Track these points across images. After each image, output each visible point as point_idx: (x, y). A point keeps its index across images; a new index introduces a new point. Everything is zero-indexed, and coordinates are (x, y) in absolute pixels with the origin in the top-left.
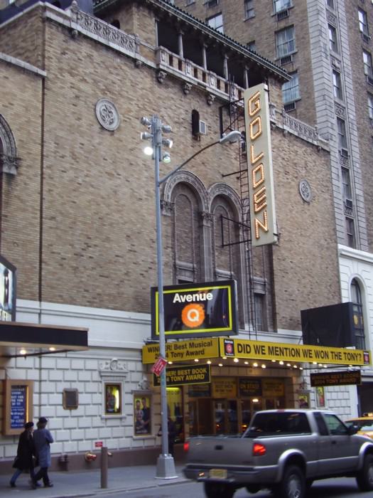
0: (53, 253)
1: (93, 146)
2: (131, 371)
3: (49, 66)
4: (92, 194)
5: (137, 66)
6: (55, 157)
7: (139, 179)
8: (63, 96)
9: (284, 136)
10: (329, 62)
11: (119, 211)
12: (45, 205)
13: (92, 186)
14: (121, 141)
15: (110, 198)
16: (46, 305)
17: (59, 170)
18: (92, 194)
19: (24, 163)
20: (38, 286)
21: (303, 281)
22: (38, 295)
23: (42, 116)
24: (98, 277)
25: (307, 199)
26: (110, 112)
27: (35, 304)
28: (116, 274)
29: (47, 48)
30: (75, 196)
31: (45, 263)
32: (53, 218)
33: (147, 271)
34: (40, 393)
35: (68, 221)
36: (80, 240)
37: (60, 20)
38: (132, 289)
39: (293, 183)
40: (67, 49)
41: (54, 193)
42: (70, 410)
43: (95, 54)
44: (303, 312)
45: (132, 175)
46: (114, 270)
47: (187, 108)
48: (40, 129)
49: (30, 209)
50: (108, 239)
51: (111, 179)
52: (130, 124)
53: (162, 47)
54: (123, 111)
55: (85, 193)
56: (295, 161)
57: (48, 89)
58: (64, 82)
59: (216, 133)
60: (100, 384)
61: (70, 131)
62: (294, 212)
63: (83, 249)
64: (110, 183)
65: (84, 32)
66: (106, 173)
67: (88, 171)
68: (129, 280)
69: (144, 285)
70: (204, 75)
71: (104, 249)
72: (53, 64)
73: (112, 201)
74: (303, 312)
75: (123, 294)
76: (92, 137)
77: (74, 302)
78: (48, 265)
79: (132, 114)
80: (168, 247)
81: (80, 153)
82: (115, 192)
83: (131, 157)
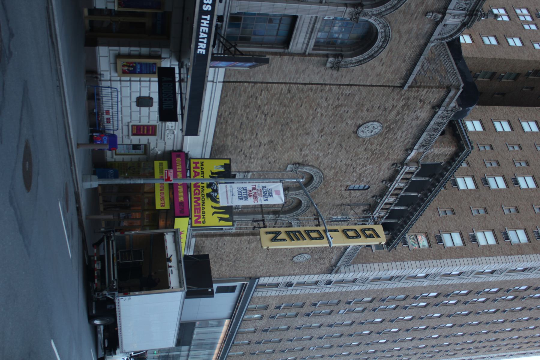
0: (262, 91)
2: (165, 143)
3: (411, 91)
4: (308, 118)
6: (338, 94)
7: (317, 150)
8: (387, 100)
10: (400, 274)
11: (292, 136)
12: (300, 86)
13: (314, 118)
14: (348, 138)
15: (303, 130)
16: (220, 86)
17: (328, 96)
18: (308, 118)
19: (335, 72)
20: (235, 80)
21: (231, 255)
22: (228, 80)
23: (372, 86)
24: (241, 121)
25: (295, 259)
26: (372, 132)
27: (221, 78)
28: (243, 133)
29: (426, 90)
30: (306, 107)
31: (254, 86)
32: (289, 91)
33: (244, 154)
34: (150, 81)
35: (286, 102)
36: (271, 109)
37: (447, 100)
38: (230, 144)
40: (424, 103)
41: (310, 92)
42: (136, 102)
43: (419, 122)
44: (207, 256)
45: (320, 145)
46: (246, 133)
47: (371, 182)
48: (362, 84)
49: (298, 76)
50: (270, 129)
51: (318, 131)
52: (361, 145)
53: (420, 168)
54: (372, 140)
55: (308, 113)
56: (325, 252)
57: (393, 90)
58: (398, 100)
59: (350, 201)
61: (359, 104)
64: (315, 130)
65: (437, 116)
66: (324, 128)
67: (326, 115)
68: (237, 142)
69: (233, 152)
70: (397, 195)
71: (263, 126)
72: (413, 94)
73: (301, 131)
74: (208, 255)
75: (227, 138)
76: (353, 119)
78: (252, 88)
79: (369, 146)
81: (340, 111)
82: (308, 134)
83: (335, 145)
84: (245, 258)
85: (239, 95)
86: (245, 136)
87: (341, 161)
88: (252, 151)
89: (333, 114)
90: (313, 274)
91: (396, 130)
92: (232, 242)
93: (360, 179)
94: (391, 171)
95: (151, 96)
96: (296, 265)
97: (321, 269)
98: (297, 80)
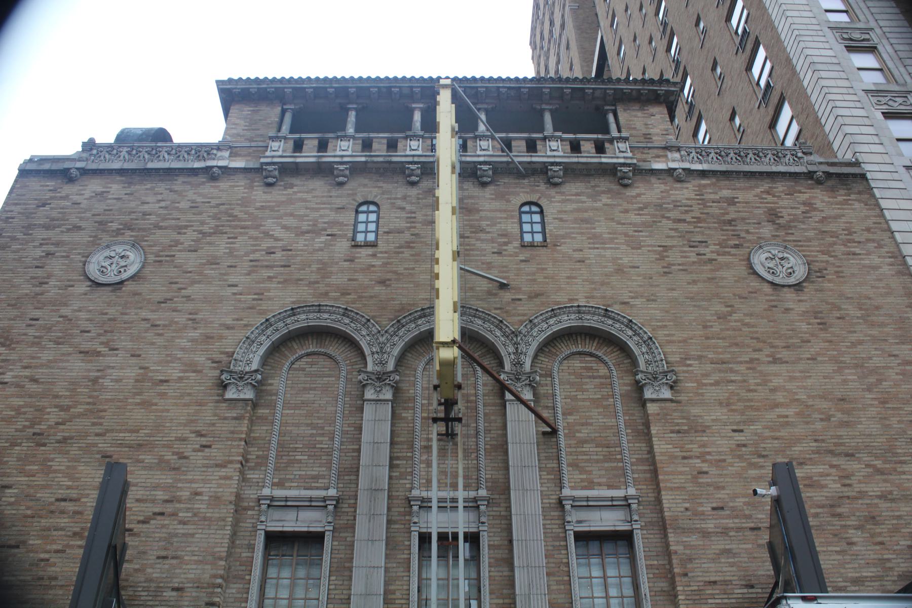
1: (60, 317)
5: (214, 178)
9: (679, 180)
26: (122, 257)
39: (720, 258)
45: (153, 344)
51: (90, 361)
56: (727, 217)
62: (735, 316)
79: (180, 247)
80: (231, 462)
81: (25, 334)
84: (819, 426)
86: (62, 529)
87: (236, 286)
88: (138, 500)
89: (33, 344)
90: (883, 216)
91: (133, 216)
92: (700, 485)
96: (831, 269)
97: (846, 202)
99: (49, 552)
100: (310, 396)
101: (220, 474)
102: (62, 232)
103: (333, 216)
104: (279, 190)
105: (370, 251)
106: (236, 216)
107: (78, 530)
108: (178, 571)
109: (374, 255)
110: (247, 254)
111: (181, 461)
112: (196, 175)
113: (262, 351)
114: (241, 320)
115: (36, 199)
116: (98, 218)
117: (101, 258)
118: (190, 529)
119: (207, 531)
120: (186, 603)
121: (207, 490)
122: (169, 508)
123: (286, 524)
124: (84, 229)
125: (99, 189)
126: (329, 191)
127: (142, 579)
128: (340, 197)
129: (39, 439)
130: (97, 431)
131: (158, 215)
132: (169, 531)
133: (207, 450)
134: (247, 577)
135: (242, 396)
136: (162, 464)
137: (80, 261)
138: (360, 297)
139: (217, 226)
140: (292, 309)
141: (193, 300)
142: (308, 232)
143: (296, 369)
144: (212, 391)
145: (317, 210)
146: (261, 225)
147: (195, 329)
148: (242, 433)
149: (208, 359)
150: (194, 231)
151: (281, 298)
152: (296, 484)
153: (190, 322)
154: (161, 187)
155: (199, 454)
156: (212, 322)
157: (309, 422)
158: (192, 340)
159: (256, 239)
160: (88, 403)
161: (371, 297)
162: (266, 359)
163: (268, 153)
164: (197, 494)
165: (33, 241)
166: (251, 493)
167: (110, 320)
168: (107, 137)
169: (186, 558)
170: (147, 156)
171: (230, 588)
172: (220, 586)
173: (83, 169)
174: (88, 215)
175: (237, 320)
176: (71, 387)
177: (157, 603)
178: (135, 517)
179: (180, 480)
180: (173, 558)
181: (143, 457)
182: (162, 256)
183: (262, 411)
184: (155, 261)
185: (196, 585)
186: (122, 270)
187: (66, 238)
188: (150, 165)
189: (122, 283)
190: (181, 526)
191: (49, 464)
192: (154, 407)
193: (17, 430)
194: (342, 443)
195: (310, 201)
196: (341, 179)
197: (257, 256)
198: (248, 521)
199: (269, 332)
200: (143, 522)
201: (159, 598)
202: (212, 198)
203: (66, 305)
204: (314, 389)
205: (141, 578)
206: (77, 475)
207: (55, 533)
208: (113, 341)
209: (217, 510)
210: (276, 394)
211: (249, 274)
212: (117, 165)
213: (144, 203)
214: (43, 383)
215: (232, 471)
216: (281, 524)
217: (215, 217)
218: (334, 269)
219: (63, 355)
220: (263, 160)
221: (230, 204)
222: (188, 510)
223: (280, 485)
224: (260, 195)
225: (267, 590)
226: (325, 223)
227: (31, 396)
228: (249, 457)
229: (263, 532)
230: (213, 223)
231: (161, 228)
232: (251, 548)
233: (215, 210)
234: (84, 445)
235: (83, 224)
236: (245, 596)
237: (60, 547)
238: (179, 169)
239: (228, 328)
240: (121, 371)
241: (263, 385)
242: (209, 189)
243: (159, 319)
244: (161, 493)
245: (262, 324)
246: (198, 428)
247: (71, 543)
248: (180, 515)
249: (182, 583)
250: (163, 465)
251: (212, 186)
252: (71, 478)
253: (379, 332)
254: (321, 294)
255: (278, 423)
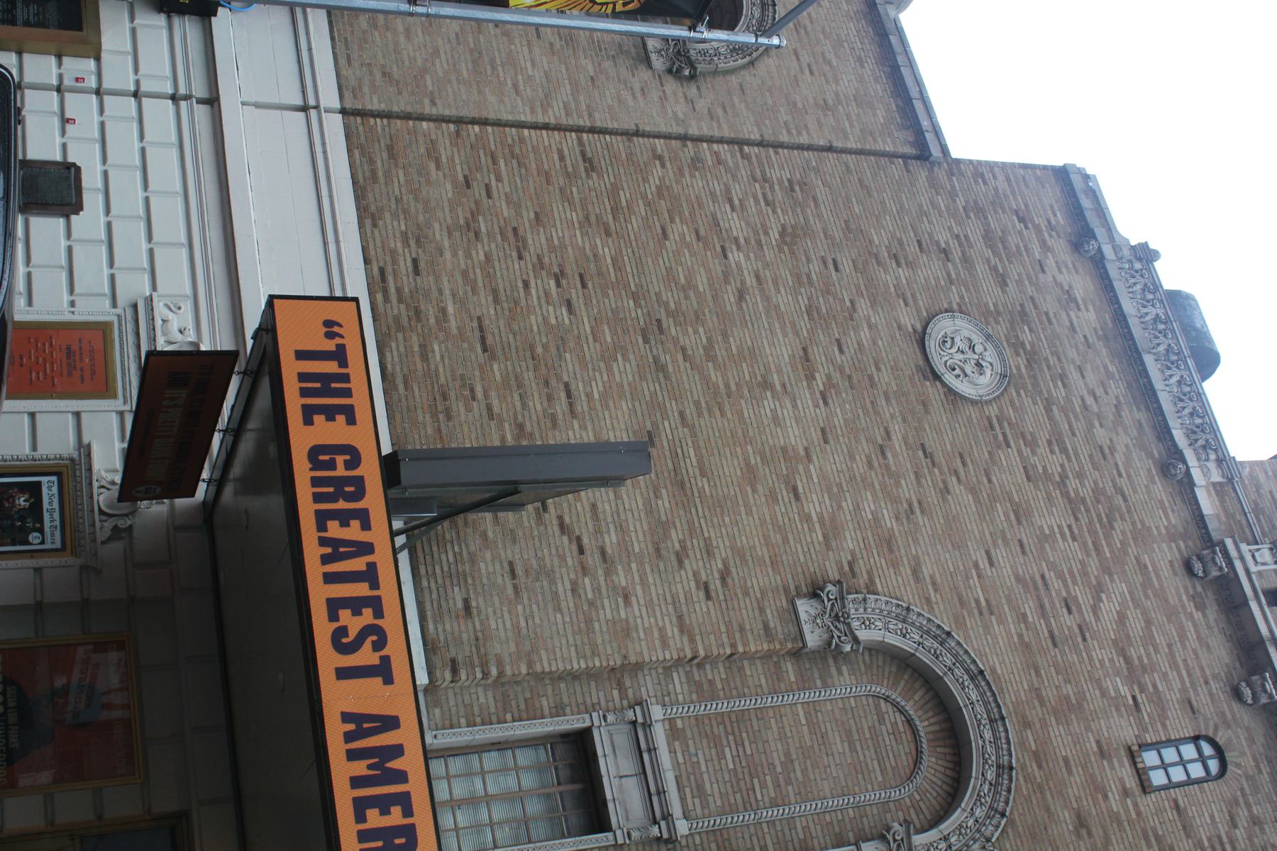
0: (495, 162)
1: (852, 301)
16: (334, 124)
19: (692, 90)
20: (383, 107)
26: (978, 365)
45: (852, 457)
48: (804, 139)
51: (794, 369)
60: (107, 303)
63: (540, 258)
77: (368, 222)
79: (1026, 451)
80: (692, 640)
81: (808, 260)
85: (420, 174)
86: (524, 405)
87: (991, 564)
88: (594, 506)
89: (797, 278)
93: (1142, 689)
94: (1213, 612)
95: (70, 160)
98: (590, 115)
99: (486, 396)
100: (838, 745)
101: (668, 626)
102: (988, 261)
103: (1173, 698)
104: (1186, 588)
105: (1131, 782)
106: (1112, 528)
107: (528, 428)
108: (496, 599)
109: (1126, 793)
110: (1052, 566)
111: (673, 558)
112: (1159, 439)
113: (894, 640)
114: (936, 590)
115: (1026, 205)
116: (1029, 307)
117: (966, 333)
118: (568, 602)
119: (569, 631)
120: (448, 627)
121: (637, 613)
122: (593, 559)
123: (610, 759)
124: (1004, 292)
125: (1079, 294)
126: (1215, 677)
127: (472, 549)
128: (1212, 702)
129: (653, 330)
130: (688, 412)
131: (1068, 399)
132: (557, 569)
133: (702, 594)
134: (509, 716)
135: (806, 628)
136: (660, 529)
137: (950, 303)
138: (1040, 787)
139: (1083, 501)
140: (981, 672)
141: (945, 500)
142: (1127, 660)
143: (877, 707)
144: (801, 576)
145: (1174, 665)
146: (1110, 575)
147: (897, 518)
148: (744, 645)
149: (853, 553)
150: (1062, 466)
151: (994, 647)
152: (681, 760)
153: (905, 505)
154: (1118, 389)
155: (693, 584)
156: (916, 541)
157: (794, 756)
158: (876, 519)
159: (1085, 574)
160: (727, 386)
161: (1048, 809)
162: (880, 651)
163: (1245, 548)
164: (626, 598)
165: (959, 223)
166: (647, 686)
167: (871, 378)
168: (1170, 275)
169: (520, 608)
170: (1161, 348)
171: (485, 691)
172: (486, 675)
173: (1103, 257)
174: (1030, 290)
175: (934, 584)
176: (746, 352)
177: (440, 581)
178: (566, 510)
179: (641, 564)
180: (515, 587)
181: (665, 496)
182: (1001, 427)
183: (789, 667)
184: (989, 419)
185: (480, 634)
186: (957, 371)
187: (980, 268)
188: (1148, 360)
189: (937, 377)
190: (568, 587)
191: (619, 357)
192: (749, 489)
193: (658, 295)
194: (771, 823)
195: (1184, 647)
196: (1247, 692)
197: (1056, 584)
198: (601, 694)
199: (929, 643)
200: (562, 526)
201: (448, 583)
202: (1129, 476)
203: (873, 303)
204: (853, 749)
205: (474, 544)
206: (611, 403)
207: (516, 397)
208: (838, 393)
209: (607, 637)
210: (825, 685)
211: (1018, 579)
212: (1128, 306)
213: (1080, 369)
214: (741, 307)
215: (678, 645)
216: (608, 750)
217: (1098, 492)
218: (1076, 727)
219: (793, 324)
220: (1229, 542)
221: (1129, 511)
222: (596, 590)
223: (674, 733)
224: (1164, 556)
225: (494, 754)
226: (1155, 686)
227: (715, 298)
228: (708, 667)
229: (588, 724)
230: (1087, 492)
231: (1048, 410)
232: (559, 710)
233: (1110, 489)
234: (660, 399)
235: (1012, 288)
236: (478, 720)
237: (496, 410)
238: (1160, 407)
239: (916, 572)
240: (792, 421)
241: (835, 658)
242: (1143, 466)
243: (895, 456)
244: (614, 540)
245: (939, 627)
246: (733, 570)
247: (506, 425)
248: (587, 580)
249: (479, 613)
250: (661, 531)
251: (1149, 470)
252: (605, 396)
253: (988, 840)
254: (1024, 716)
255: (777, 700)
